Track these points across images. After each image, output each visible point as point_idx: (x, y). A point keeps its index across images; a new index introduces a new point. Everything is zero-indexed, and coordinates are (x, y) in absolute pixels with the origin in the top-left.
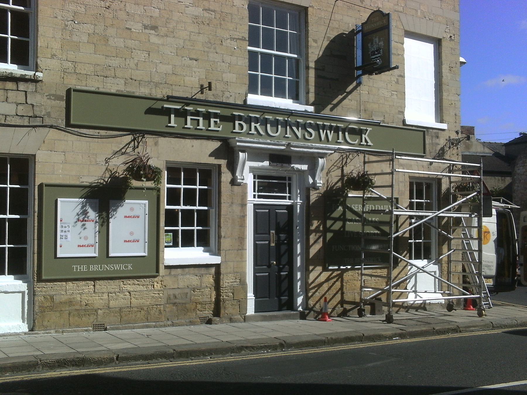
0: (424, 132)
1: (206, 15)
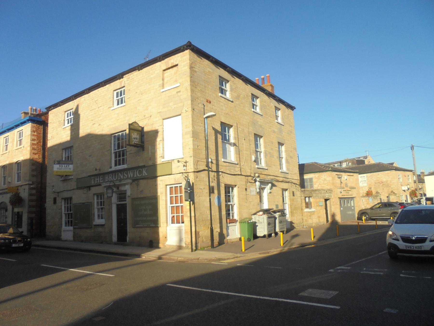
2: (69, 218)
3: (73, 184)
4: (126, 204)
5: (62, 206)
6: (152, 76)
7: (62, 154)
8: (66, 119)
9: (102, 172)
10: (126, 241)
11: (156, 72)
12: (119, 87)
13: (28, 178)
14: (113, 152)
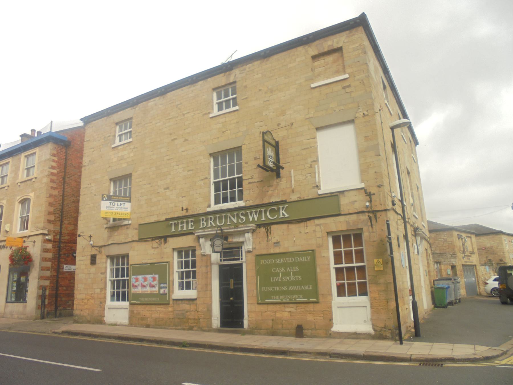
0: (337, 195)
1: (189, 173)
2: (118, 288)
3: (132, 234)
4: (241, 265)
5: (106, 268)
6: (290, 66)
7: (110, 186)
8: (118, 134)
9: (190, 213)
10: (242, 326)
11: (298, 60)
12: (224, 84)
13: (41, 225)
14: (212, 183)
